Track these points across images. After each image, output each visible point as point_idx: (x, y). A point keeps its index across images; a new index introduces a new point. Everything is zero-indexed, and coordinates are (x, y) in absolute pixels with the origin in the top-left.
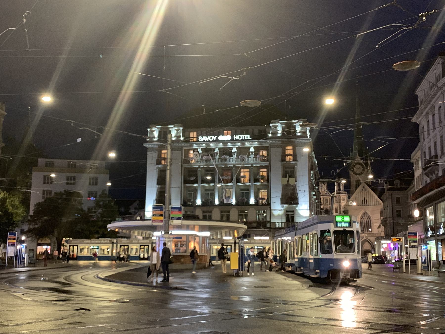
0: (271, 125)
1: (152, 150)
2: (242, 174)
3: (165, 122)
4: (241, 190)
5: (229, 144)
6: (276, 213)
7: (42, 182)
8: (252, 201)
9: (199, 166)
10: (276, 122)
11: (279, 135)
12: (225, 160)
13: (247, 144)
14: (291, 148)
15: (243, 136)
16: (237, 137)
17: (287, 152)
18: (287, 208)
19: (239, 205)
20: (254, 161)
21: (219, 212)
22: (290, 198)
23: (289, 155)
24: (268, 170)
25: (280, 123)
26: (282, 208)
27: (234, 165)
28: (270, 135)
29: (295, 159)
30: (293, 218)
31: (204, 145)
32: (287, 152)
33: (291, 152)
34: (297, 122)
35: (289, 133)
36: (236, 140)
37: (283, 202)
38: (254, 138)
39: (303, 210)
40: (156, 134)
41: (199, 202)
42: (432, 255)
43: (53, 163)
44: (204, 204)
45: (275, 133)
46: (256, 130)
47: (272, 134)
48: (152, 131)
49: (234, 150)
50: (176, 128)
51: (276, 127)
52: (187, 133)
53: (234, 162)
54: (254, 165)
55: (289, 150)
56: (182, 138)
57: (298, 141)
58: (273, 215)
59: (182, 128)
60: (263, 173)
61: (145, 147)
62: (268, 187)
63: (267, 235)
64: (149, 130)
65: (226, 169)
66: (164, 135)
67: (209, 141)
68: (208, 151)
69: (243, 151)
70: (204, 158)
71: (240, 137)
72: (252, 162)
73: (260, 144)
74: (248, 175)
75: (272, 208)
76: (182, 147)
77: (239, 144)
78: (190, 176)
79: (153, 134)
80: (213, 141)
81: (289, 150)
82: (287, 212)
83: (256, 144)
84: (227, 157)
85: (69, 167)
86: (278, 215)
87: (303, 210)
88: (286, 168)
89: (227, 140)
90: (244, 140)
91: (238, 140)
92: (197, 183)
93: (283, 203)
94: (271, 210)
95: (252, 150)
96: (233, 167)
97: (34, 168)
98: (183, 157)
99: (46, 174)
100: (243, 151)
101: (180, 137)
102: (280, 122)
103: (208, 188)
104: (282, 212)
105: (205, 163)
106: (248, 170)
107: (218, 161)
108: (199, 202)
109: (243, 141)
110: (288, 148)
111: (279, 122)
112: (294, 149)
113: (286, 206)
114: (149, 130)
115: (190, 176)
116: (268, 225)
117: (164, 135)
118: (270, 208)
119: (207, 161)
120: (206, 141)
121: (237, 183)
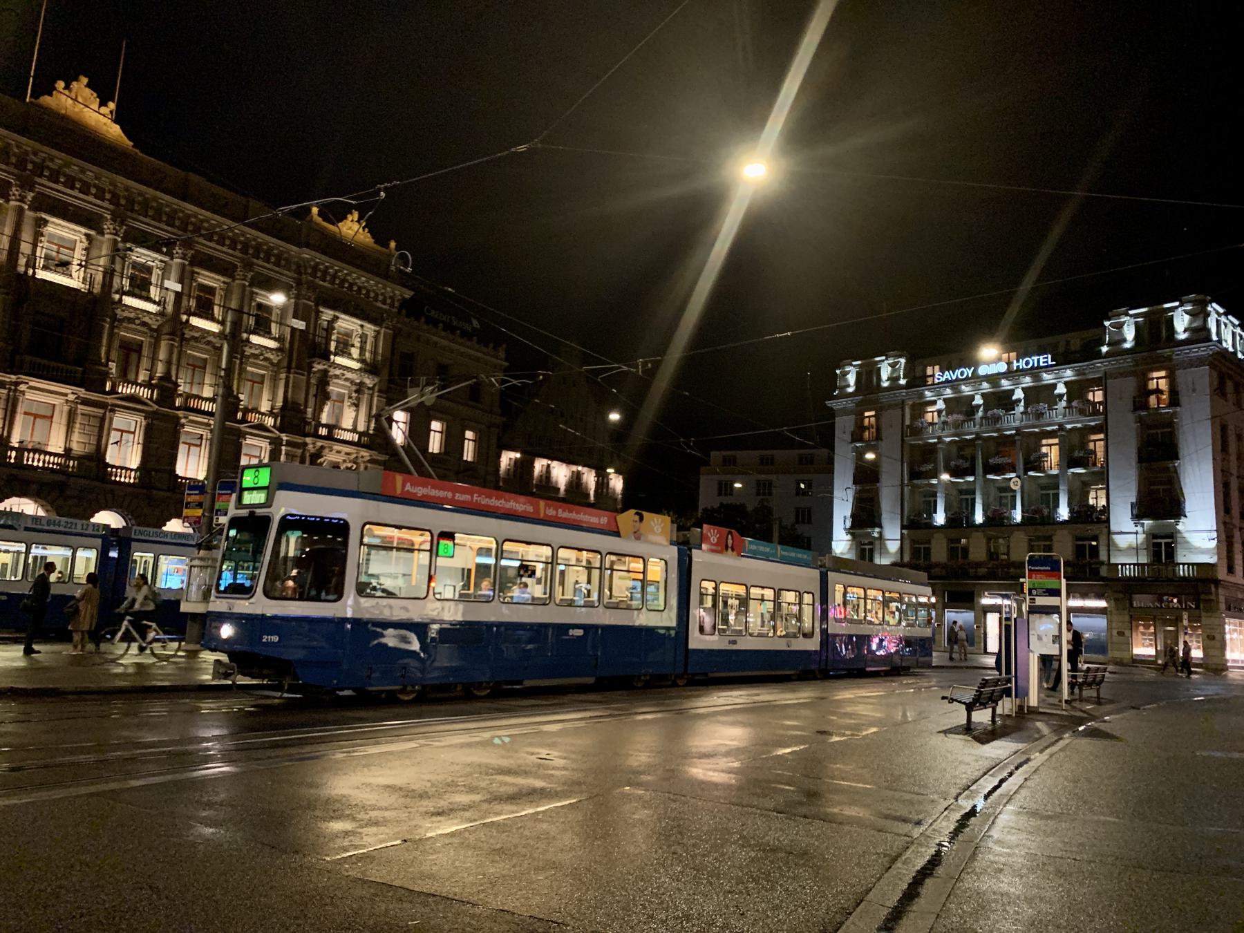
0: (1107, 323)
1: (845, 412)
2: (1044, 450)
3: (867, 354)
4: (1043, 488)
5: (1004, 382)
6: (1122, 541)
7: (716, 491)
8: (1063, 513)
9: (939, 438)
10: (1119, 315)
11: (1128, 345)
12: (997, 419)
13: (1047, 378)
14: (1163, 373)
15: (1035, 358)
16: (1022, 364)
17: (1152, 385)
18: (1152, 527)
19: (1076, 523)
20: (1065, 416)
21: (984, 541)
22: (1161, 502)
23: (1158, 391)
24: (1106, 436)
25: (1131, 316)
26: (1139, 529)
27: (1017, 429)
28: (1105, 349)
29: (1174, 401)
30: (1171, 553)
31: (948, 391)
32: (1152, 385)
33: (1163, 384)
34: (1177, 307)
35: (1156, 333)
36: (1018, 369)
37: (1140, 513)
38: (1062, 359)
39: (1199, 533)
40: (851, 378)
41: (940, 518)
42: (989, 641)
43: (735, 458)
44: (952, 521)
45: (1118, 341)
46: (1075, 340)
47: (1108, 345)
48: (845, 374)
49: (1019, 394)
50: (891, 361)
51: (1120, 326)
52: (919, 369)
53: (1017, 423)
54: (1069, 426)
55: (1159, 380)
56: (903, 382)
57: (1179, 354)
58: (1116, 545)
59: (903, 361)
60: (1097, 444)
61: (832, 409)
62: (1102, 477)
63: (1099, 596)
64: (838, 372)
65: (1005, 443)
66: (868, 378)
67: (957, 380)
68: (961, 406)
69: (1040, 395)
70: (950, 419)
71: (1027, 363)
72: (1060, 419)
73: (1079, 373)
74: (1055, 449)
75: (1113, 528)
76: (903, 402)
77: (1028, 379)
78: (920, 461)
79: (846, 380)
80: (967, 378)
81: (1159, 380)
82: (1155, 536)
83: (1069, 374)
84: (1001, 412)
85: (762, 463)
86: (1130, 548)
87: (1199, 533)
88: (1149, 427)
89: (999, 374)
90: (1039, 367)
91: (1023, 370)
92: (973, 474)
93: (1138, 516)
94: (1109, 533)
95: (1061, 389)
96: (1016, 434)
97: (703, 469)
98: (907, 422)
99: (723, 477)
100: (1040, 395)
101: (898, 378)
102: (1131, 312)
103: (965, 487)
104: (1141, 537)
105: (953, 431)
106: (1056, 441)
107: (981, 425)
108: (940, 518)
109: (1035, 372)
110: (1156, 374)
111: (1127, 314)
112: (1171, 378)
113: (1148, 523)
114: (838, 372)
115: (920, 461)
116: (1104, 571)
117: (868, 378)
118: (1109, 527)
119: (958, 425)
120: (952, 381)
121: (1025, 473)
